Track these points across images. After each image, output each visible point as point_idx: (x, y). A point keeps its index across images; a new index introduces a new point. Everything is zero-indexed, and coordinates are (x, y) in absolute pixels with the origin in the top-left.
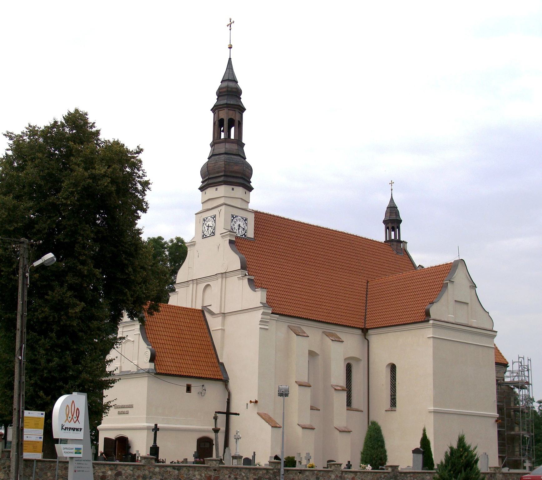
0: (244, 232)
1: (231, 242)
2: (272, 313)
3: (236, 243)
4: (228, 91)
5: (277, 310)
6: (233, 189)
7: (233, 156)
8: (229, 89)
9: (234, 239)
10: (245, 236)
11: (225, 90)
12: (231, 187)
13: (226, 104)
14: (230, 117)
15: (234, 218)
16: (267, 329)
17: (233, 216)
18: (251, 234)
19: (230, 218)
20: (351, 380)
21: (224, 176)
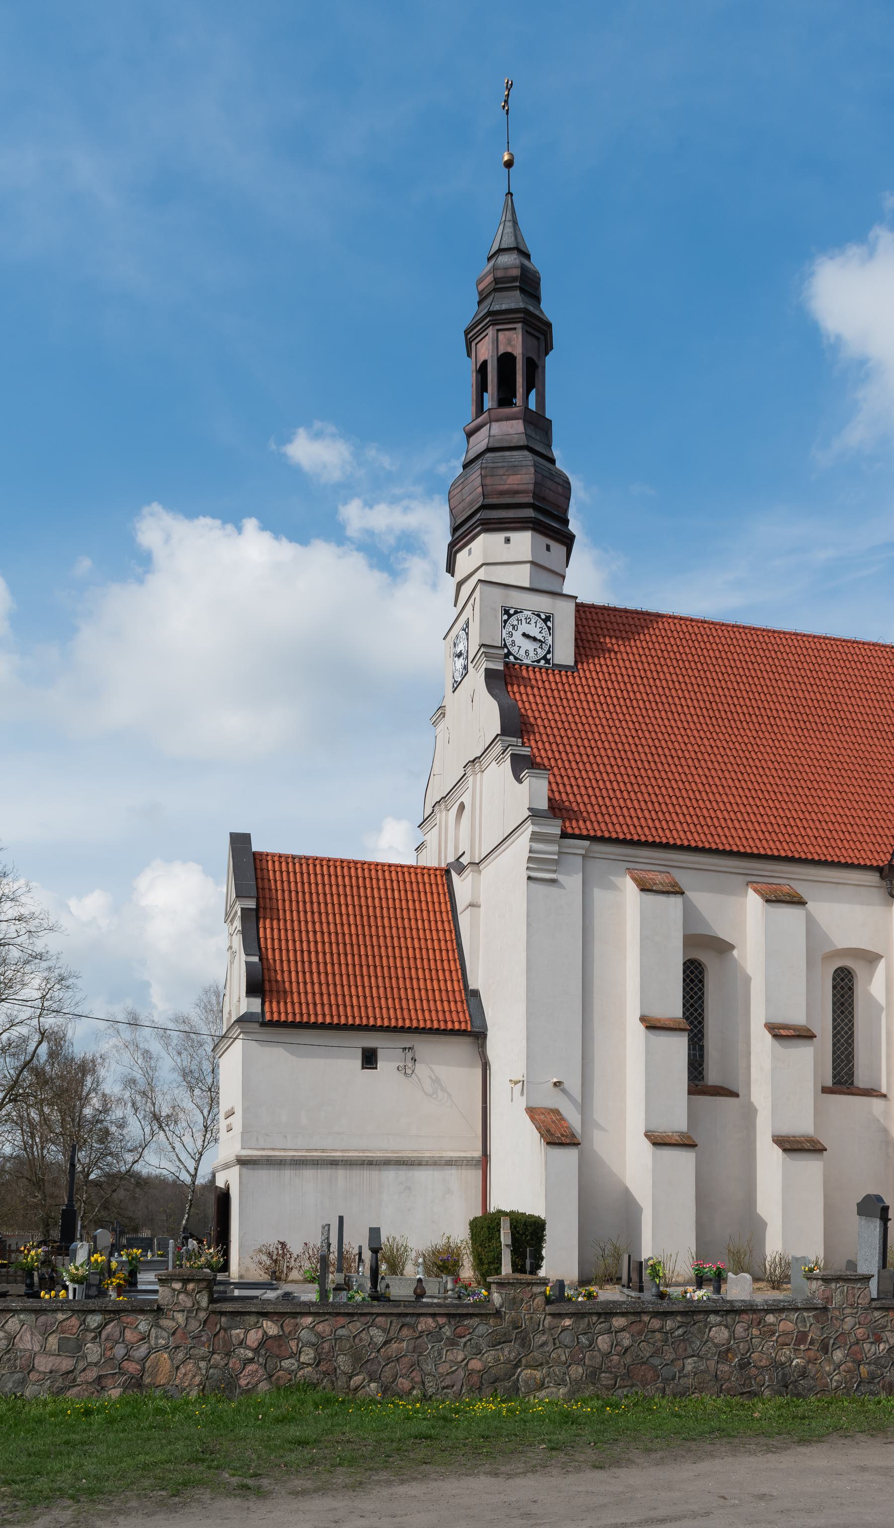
0: (541, 653)
1: (490, 675)
2: (564, 835)
3: (504, 678)
4: (496, 280)
5: (583, 828)
6: (508, 540)
7: (507, 453)
8: (499, 274)
9: (501, 667)
10: (547, 661)
11: (490, 279)
12: (500, 537)
13: (490, 313)
14: (501, 352)
15: (510, 616)
16: (553, 881)
17: (506, 612)
18: (565, 654)
19: (500, 617)
20: (851, 1013)
21: (484, 507)
